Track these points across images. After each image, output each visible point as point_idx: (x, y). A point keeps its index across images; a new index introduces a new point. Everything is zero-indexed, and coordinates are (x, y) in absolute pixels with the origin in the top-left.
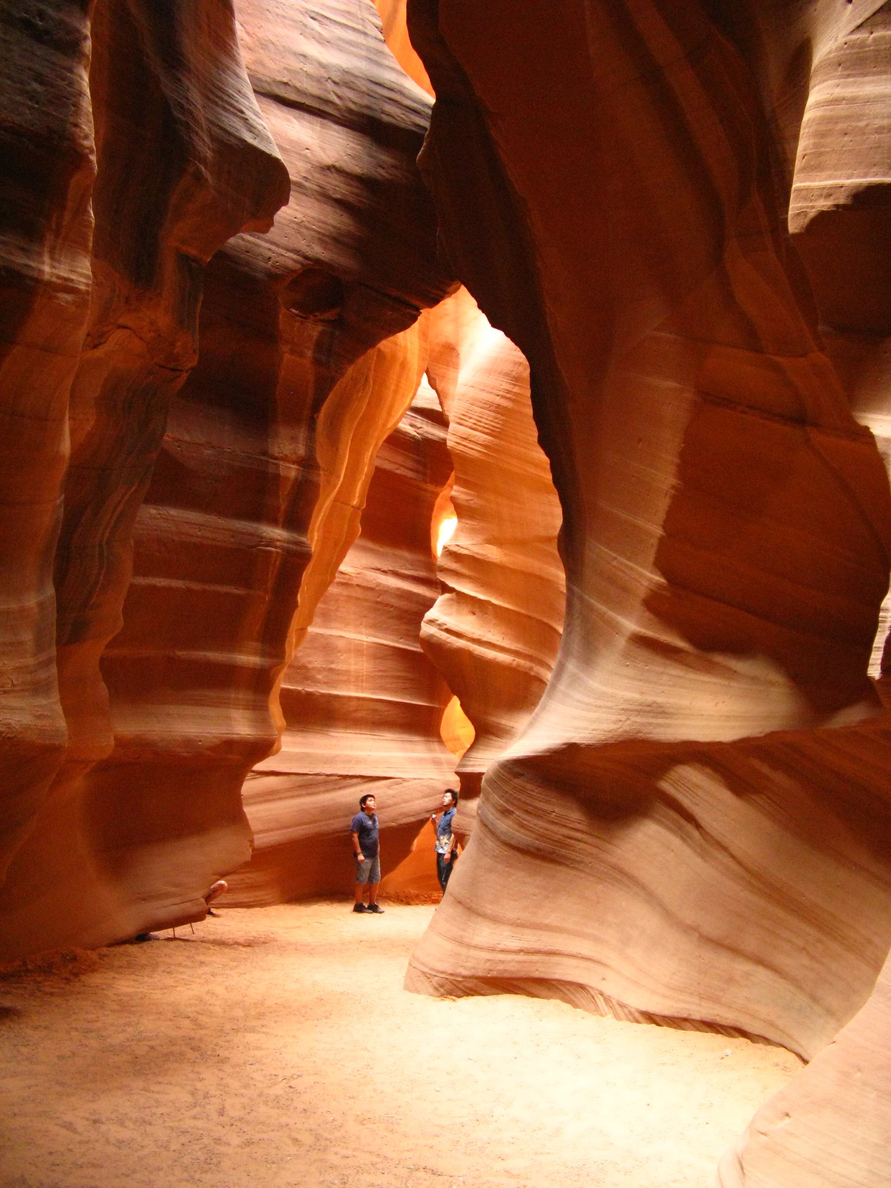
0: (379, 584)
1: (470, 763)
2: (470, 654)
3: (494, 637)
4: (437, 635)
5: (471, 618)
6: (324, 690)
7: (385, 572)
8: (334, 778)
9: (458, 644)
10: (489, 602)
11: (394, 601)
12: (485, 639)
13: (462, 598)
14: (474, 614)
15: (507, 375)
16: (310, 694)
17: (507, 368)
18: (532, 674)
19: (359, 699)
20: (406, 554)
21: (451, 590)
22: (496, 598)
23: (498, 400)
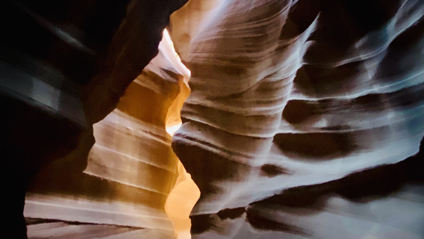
0: (144, 136)
1: (200, 209)
5: (199, 132)
6: (113, 179)
7: (146, 132)
8: (113, 227)
10: (207, 125)
11: (149, 144)
13: (193, 123)
15: (218, 26)
16: (105, 181)
17: (219, 24)
18: (230, 159)
19: (130, 186)
20: (156, 127)
23: (214, 38)
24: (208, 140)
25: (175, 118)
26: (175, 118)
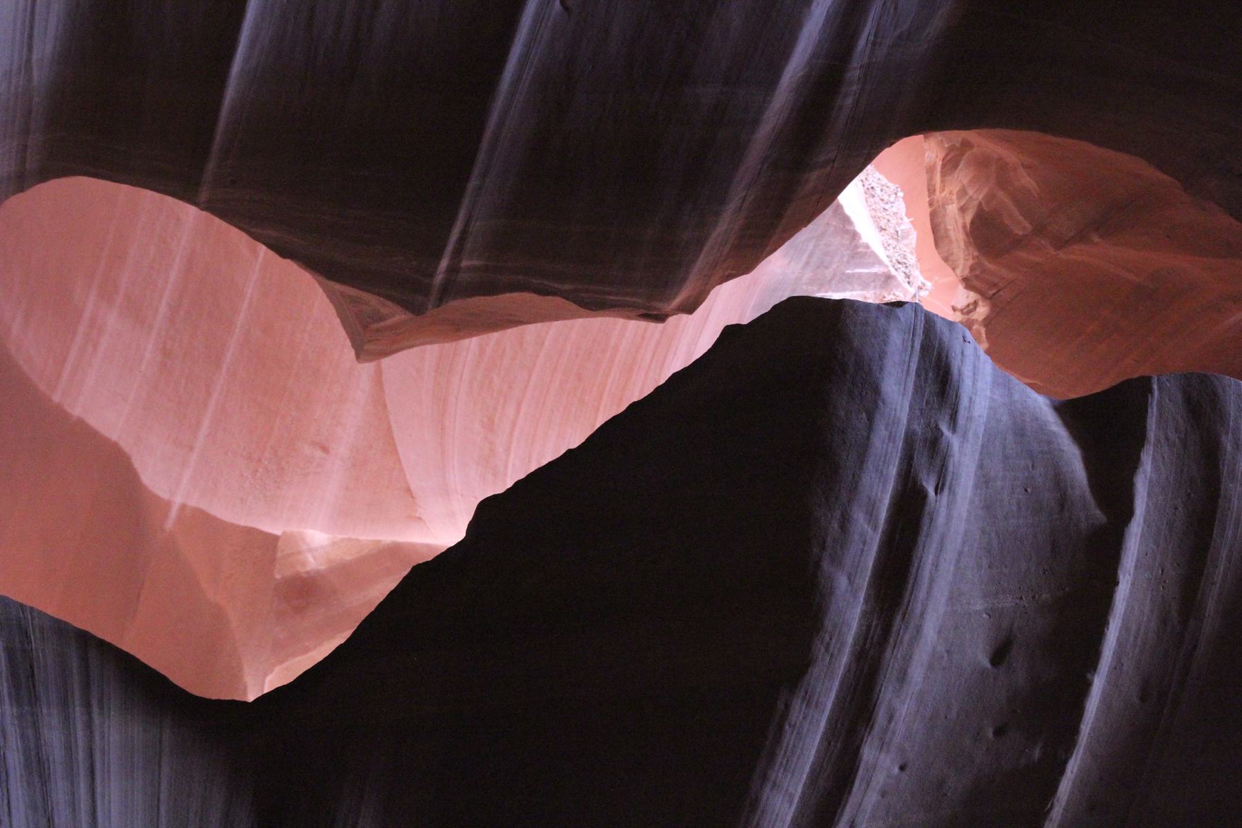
2: (794, 670)
3: (872, 798)
4: (880, 433)
9: (842, 582)
12: (868, 753)
13: (1079, 568)
14: (999, 655)
21: (1115, 497)
22: (1081, 784)
24: (880, 765)
25: (1020, 225)
26: (1020, 225)
